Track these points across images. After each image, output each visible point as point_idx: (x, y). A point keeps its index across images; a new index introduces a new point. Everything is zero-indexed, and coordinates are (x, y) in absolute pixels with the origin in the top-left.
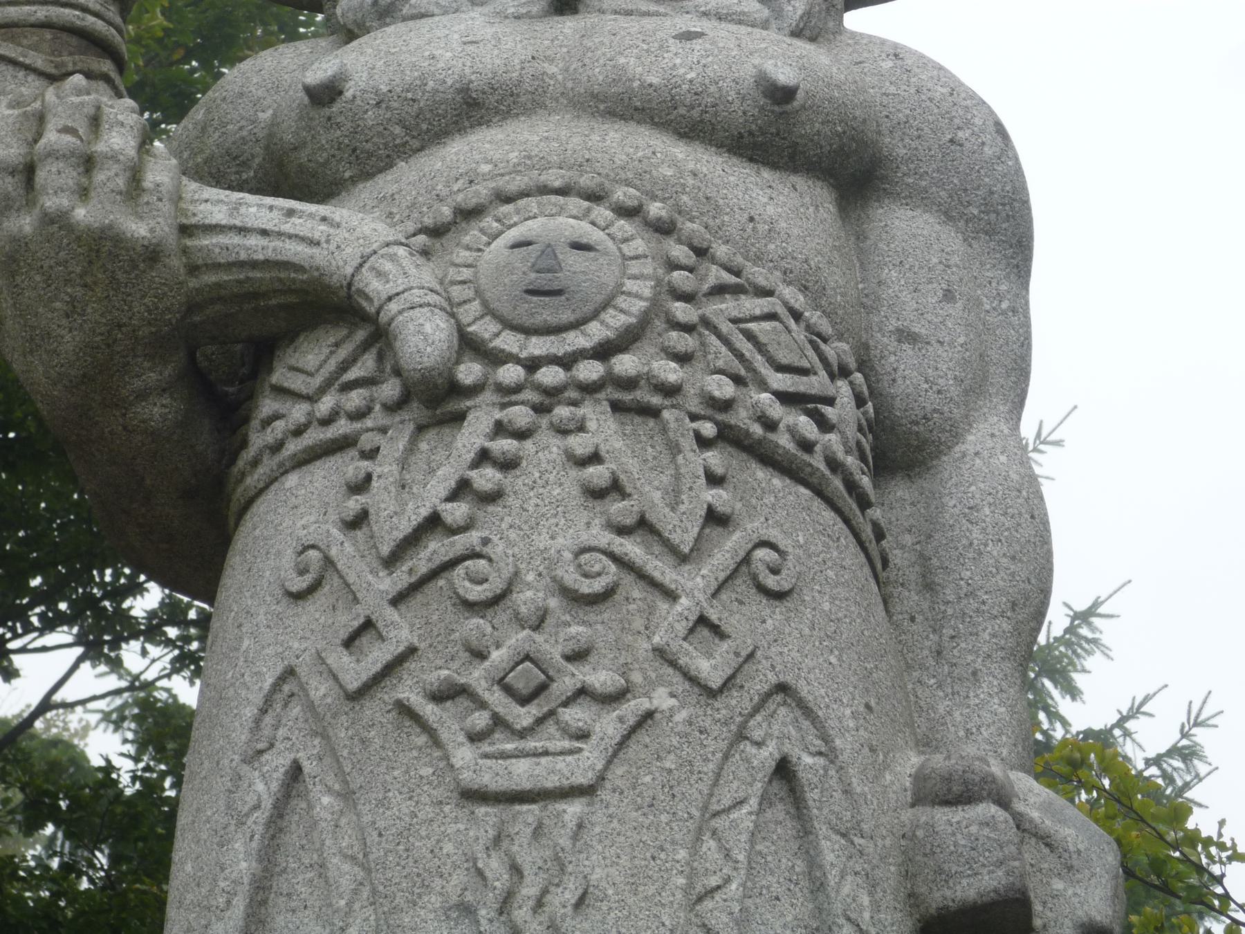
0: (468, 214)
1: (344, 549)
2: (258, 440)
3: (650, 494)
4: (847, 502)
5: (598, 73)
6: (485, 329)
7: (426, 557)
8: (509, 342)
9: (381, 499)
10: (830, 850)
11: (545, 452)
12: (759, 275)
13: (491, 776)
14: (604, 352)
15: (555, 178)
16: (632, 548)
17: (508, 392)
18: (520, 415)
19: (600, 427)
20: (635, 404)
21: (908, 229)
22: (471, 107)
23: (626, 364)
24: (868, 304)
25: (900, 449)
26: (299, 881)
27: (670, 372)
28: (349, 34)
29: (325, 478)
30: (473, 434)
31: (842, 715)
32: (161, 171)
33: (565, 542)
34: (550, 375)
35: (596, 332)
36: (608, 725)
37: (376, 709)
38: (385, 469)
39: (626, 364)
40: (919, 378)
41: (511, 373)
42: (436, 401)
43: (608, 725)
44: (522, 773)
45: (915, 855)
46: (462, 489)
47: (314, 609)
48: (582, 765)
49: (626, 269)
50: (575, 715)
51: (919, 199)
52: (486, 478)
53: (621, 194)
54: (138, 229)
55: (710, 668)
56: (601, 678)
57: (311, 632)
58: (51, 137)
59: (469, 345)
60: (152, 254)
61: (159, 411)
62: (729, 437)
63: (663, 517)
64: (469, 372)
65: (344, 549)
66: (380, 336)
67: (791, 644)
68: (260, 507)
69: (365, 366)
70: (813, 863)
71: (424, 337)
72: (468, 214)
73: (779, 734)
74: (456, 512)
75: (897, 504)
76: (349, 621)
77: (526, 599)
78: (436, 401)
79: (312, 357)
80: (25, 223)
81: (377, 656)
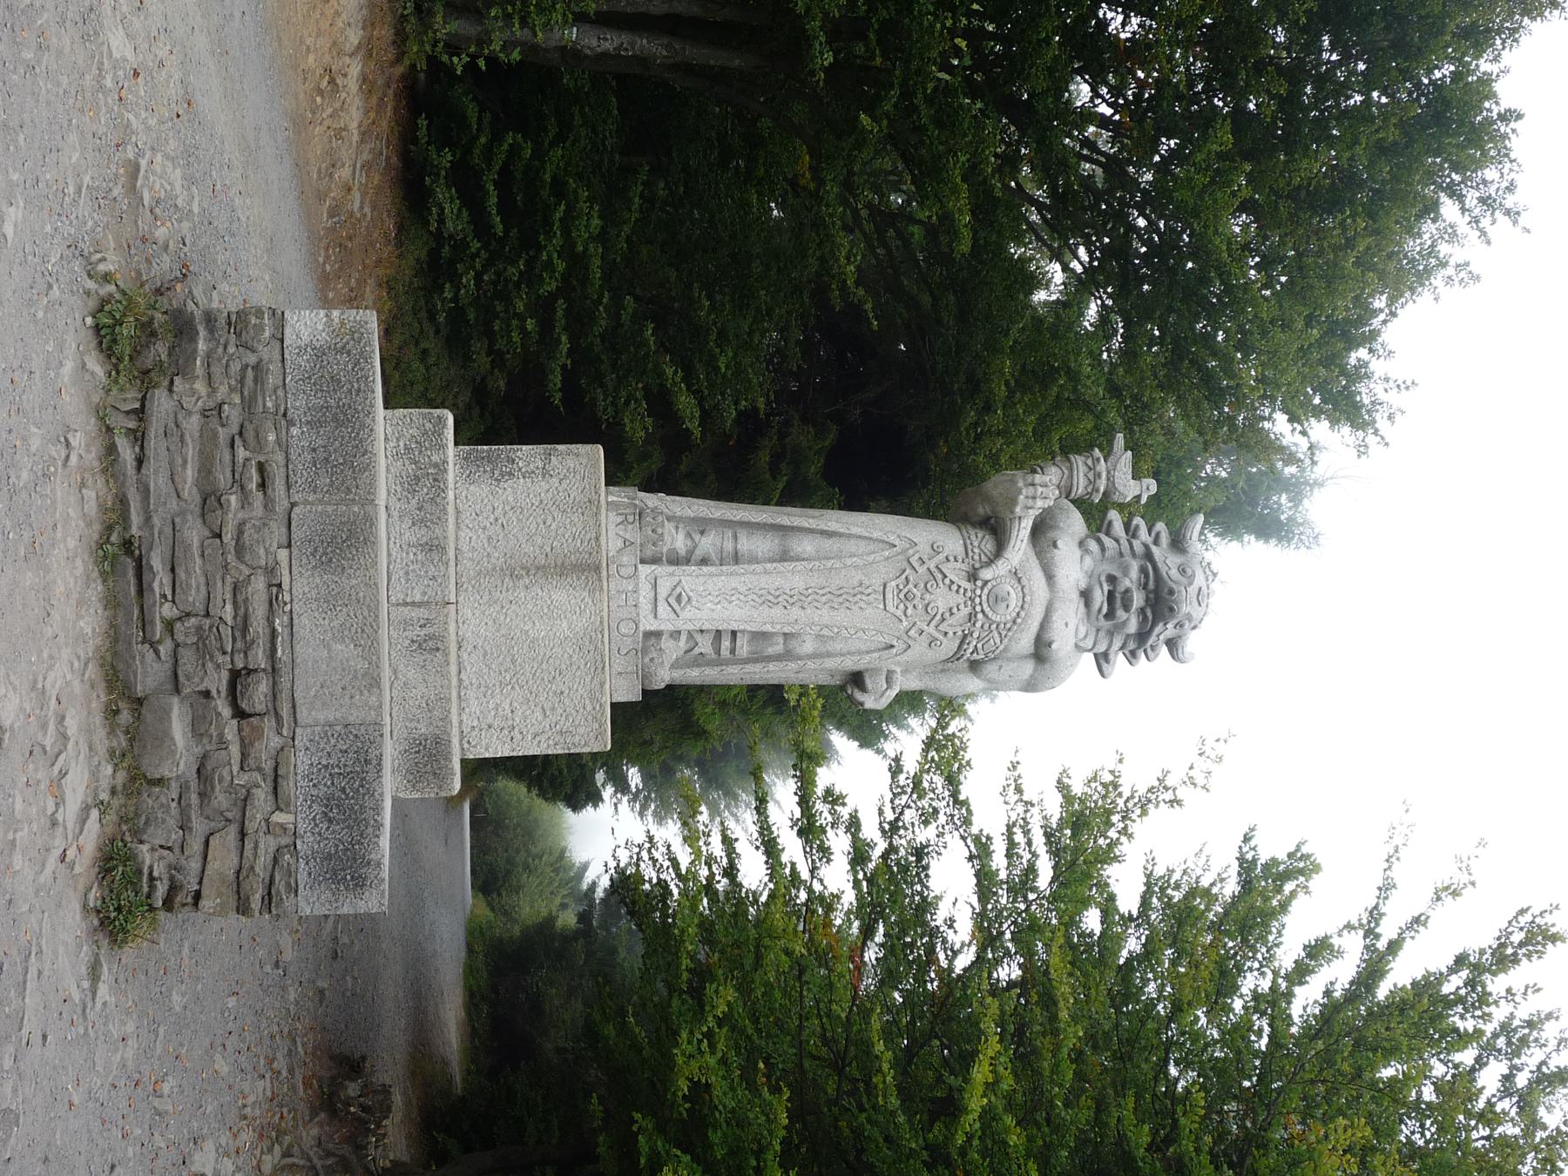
0: (1019, 580)
1: (941, 557)
2: (972, 532)
4: (957, 656)
5: (1057, 605)
6: (989, 585)
7: (937, 575)
8: (986, 591)
9: (952, 564)
10: (876, 655)
11: (960, 599)
12: (1006, 641)
15: (1028, 598)
16: (938, 617)
17: (974, 591)
18: (969, 594)
19: (965, 611)
20: (971, 617)
21: (1028, 668)
22: (1050, 577)
23: (980, 616)
24: (1008, 659)
25: (975, 666)
26: (872, 547)
27: (978, 624)
28: (1081, 544)
29: (960, 550)
30: (965, 584)
31: (905, 657)
32: (1033, 513)
33: (940, 604)
34: (977, 600)
35: (987, 610)
36: (899, 613)
37: (905, 564)
38: (959, 565)
39: (980, 616)
40: (991, 670)
41: (978, 592)
42: (973, 576)
43: (899, 613)
44: (889, 596)
45: (876, 671)
47: (929, 550)
48: (890, 608)
49: (1003, 615)
51: (1035, 670)
52: (954, 587)
53: (1023, 614)
54: (1018, 509)
55: (912, 633)
56: (909, 612)
57: (924, 549)
58: (1040, 489)
59: (986, 583)
60: (1012, 512)
61: (981, 510)
62: (965, 636)
63: (945, 623)
64: (979, 583)
65: (941, 557)
66: (990, 562)
67: (919, 649)
68: (958, 534)
69: (984, 559)
71: (986, 574)
72: (1019, 580)
73: (900, 645)
74: (947, 581)
75: (963, 664)
76: (925, 558)
77: (927, 596)
78: (973, 576)
79: (989, 545)
80: (1021, 484)
81: (916, 565)
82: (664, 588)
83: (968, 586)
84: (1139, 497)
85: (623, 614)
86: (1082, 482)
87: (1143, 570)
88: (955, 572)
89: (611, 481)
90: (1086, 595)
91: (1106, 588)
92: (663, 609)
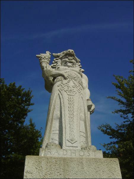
1: (62, 84)
3: (76, 84)
11: (71, 81)
13: (69, 94)
14: (74, 78)
16: (76, 86)
23: (75, 78)
36: (75, 93)
39: (75, 78)
44: (71, 94)
46: (68, 82)
48: (74, 94)
50: (73, 92)
52: (69, 82)
59: (67, 77)
64: (68, 78)
70: (83, 101)
74: (67, 83)
81: (63, 89)
82: (70, 144)
83: (68, 79)
84: (50, 54)
85: (77, 154)
86: (46, 60)
87: (64, 58)
88: (65, 81)
89: (39, 155)
90: (69, 67)
91: (68, 63)
92: (74, 145)
